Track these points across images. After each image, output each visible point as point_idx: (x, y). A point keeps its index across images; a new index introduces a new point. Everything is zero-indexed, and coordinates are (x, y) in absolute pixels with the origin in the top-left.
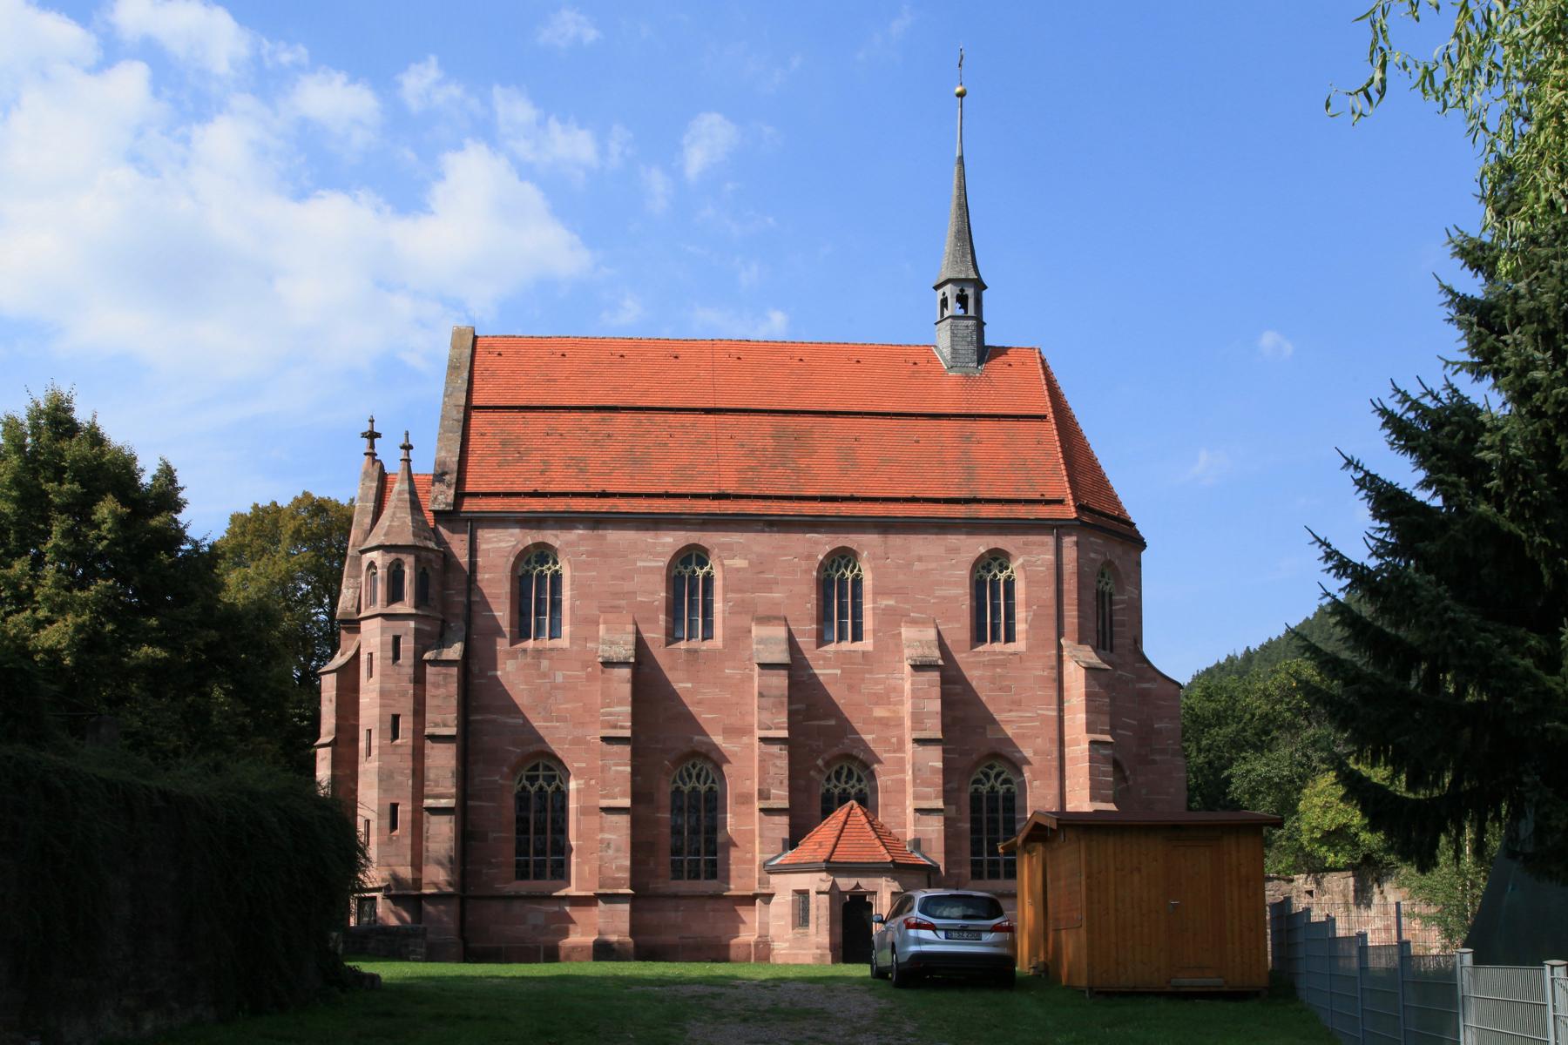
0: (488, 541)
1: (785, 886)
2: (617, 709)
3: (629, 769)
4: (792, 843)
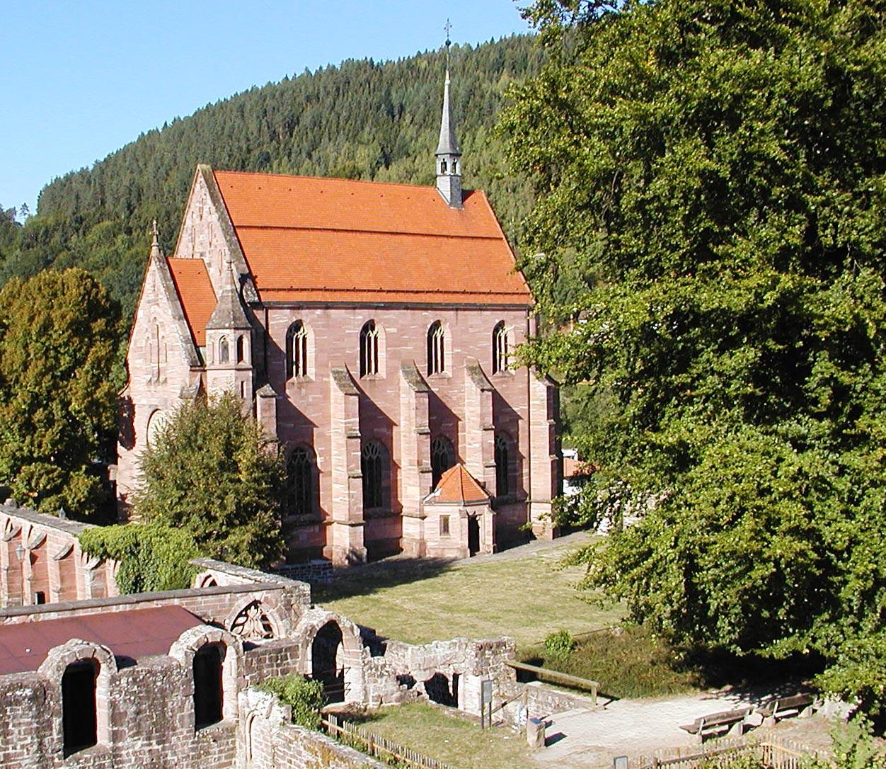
0: (274, 319)
1: (434, 513)
2: (352, 420)
3: (359, 453)
4: (433, 489)
